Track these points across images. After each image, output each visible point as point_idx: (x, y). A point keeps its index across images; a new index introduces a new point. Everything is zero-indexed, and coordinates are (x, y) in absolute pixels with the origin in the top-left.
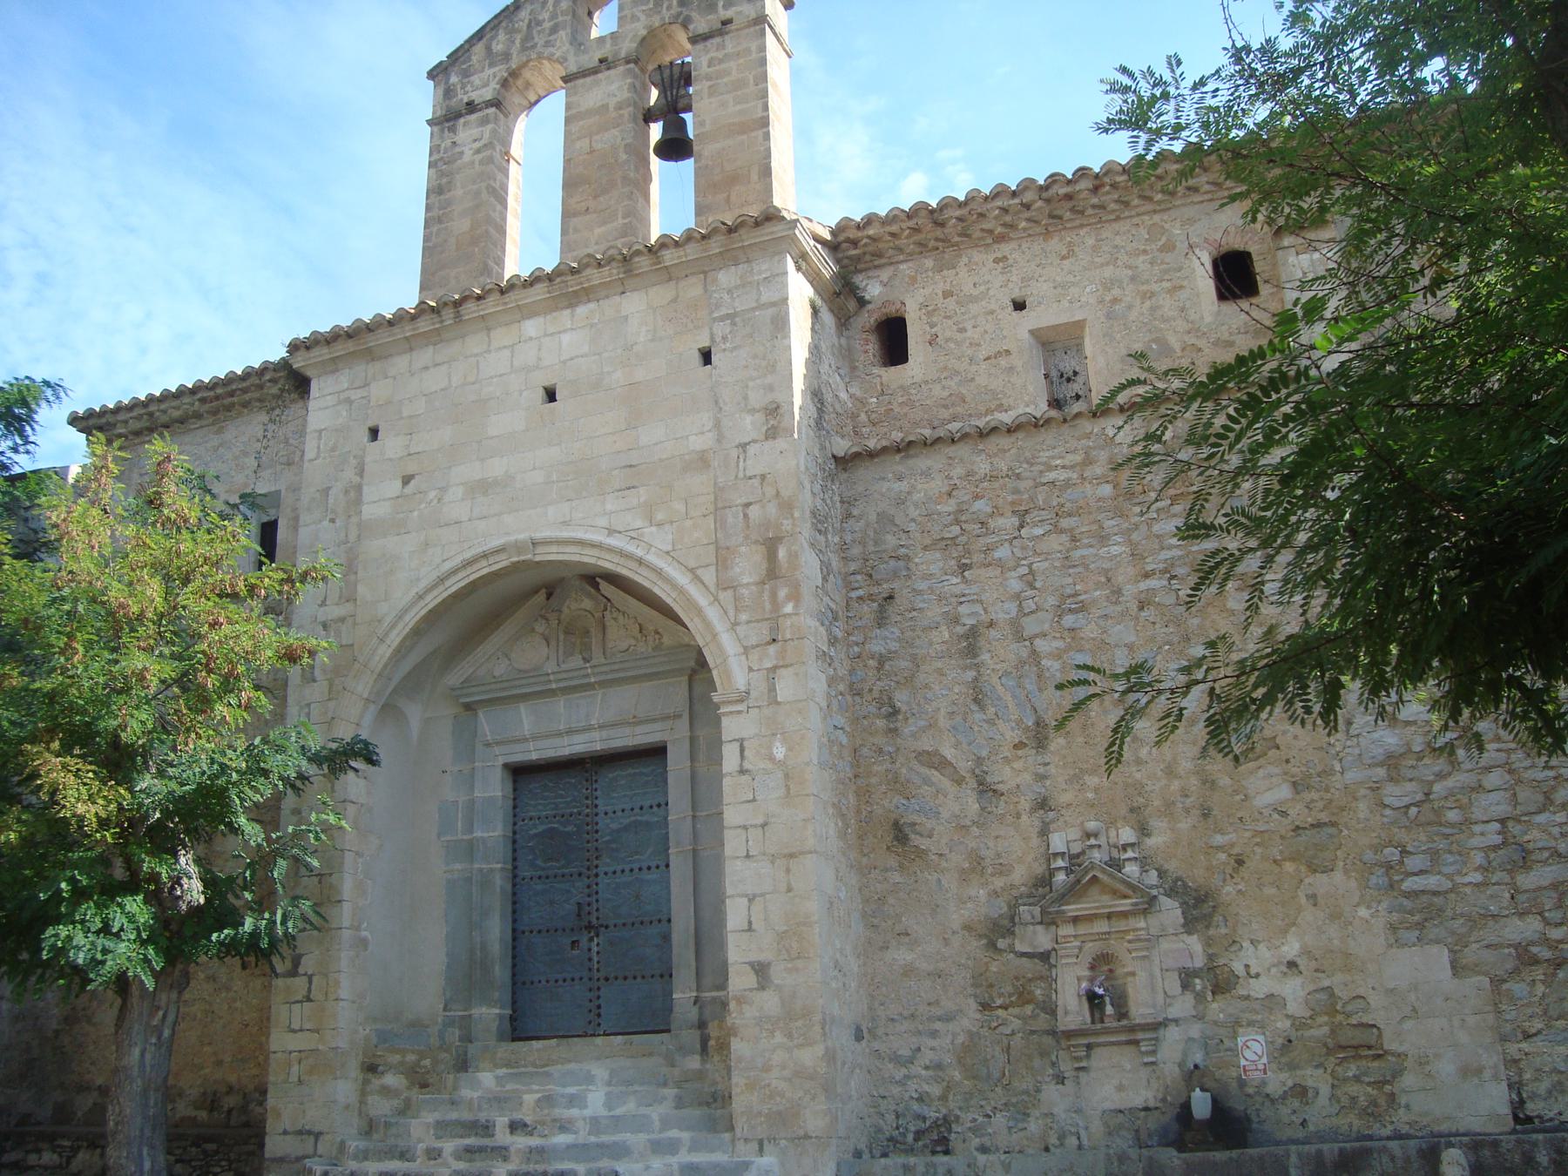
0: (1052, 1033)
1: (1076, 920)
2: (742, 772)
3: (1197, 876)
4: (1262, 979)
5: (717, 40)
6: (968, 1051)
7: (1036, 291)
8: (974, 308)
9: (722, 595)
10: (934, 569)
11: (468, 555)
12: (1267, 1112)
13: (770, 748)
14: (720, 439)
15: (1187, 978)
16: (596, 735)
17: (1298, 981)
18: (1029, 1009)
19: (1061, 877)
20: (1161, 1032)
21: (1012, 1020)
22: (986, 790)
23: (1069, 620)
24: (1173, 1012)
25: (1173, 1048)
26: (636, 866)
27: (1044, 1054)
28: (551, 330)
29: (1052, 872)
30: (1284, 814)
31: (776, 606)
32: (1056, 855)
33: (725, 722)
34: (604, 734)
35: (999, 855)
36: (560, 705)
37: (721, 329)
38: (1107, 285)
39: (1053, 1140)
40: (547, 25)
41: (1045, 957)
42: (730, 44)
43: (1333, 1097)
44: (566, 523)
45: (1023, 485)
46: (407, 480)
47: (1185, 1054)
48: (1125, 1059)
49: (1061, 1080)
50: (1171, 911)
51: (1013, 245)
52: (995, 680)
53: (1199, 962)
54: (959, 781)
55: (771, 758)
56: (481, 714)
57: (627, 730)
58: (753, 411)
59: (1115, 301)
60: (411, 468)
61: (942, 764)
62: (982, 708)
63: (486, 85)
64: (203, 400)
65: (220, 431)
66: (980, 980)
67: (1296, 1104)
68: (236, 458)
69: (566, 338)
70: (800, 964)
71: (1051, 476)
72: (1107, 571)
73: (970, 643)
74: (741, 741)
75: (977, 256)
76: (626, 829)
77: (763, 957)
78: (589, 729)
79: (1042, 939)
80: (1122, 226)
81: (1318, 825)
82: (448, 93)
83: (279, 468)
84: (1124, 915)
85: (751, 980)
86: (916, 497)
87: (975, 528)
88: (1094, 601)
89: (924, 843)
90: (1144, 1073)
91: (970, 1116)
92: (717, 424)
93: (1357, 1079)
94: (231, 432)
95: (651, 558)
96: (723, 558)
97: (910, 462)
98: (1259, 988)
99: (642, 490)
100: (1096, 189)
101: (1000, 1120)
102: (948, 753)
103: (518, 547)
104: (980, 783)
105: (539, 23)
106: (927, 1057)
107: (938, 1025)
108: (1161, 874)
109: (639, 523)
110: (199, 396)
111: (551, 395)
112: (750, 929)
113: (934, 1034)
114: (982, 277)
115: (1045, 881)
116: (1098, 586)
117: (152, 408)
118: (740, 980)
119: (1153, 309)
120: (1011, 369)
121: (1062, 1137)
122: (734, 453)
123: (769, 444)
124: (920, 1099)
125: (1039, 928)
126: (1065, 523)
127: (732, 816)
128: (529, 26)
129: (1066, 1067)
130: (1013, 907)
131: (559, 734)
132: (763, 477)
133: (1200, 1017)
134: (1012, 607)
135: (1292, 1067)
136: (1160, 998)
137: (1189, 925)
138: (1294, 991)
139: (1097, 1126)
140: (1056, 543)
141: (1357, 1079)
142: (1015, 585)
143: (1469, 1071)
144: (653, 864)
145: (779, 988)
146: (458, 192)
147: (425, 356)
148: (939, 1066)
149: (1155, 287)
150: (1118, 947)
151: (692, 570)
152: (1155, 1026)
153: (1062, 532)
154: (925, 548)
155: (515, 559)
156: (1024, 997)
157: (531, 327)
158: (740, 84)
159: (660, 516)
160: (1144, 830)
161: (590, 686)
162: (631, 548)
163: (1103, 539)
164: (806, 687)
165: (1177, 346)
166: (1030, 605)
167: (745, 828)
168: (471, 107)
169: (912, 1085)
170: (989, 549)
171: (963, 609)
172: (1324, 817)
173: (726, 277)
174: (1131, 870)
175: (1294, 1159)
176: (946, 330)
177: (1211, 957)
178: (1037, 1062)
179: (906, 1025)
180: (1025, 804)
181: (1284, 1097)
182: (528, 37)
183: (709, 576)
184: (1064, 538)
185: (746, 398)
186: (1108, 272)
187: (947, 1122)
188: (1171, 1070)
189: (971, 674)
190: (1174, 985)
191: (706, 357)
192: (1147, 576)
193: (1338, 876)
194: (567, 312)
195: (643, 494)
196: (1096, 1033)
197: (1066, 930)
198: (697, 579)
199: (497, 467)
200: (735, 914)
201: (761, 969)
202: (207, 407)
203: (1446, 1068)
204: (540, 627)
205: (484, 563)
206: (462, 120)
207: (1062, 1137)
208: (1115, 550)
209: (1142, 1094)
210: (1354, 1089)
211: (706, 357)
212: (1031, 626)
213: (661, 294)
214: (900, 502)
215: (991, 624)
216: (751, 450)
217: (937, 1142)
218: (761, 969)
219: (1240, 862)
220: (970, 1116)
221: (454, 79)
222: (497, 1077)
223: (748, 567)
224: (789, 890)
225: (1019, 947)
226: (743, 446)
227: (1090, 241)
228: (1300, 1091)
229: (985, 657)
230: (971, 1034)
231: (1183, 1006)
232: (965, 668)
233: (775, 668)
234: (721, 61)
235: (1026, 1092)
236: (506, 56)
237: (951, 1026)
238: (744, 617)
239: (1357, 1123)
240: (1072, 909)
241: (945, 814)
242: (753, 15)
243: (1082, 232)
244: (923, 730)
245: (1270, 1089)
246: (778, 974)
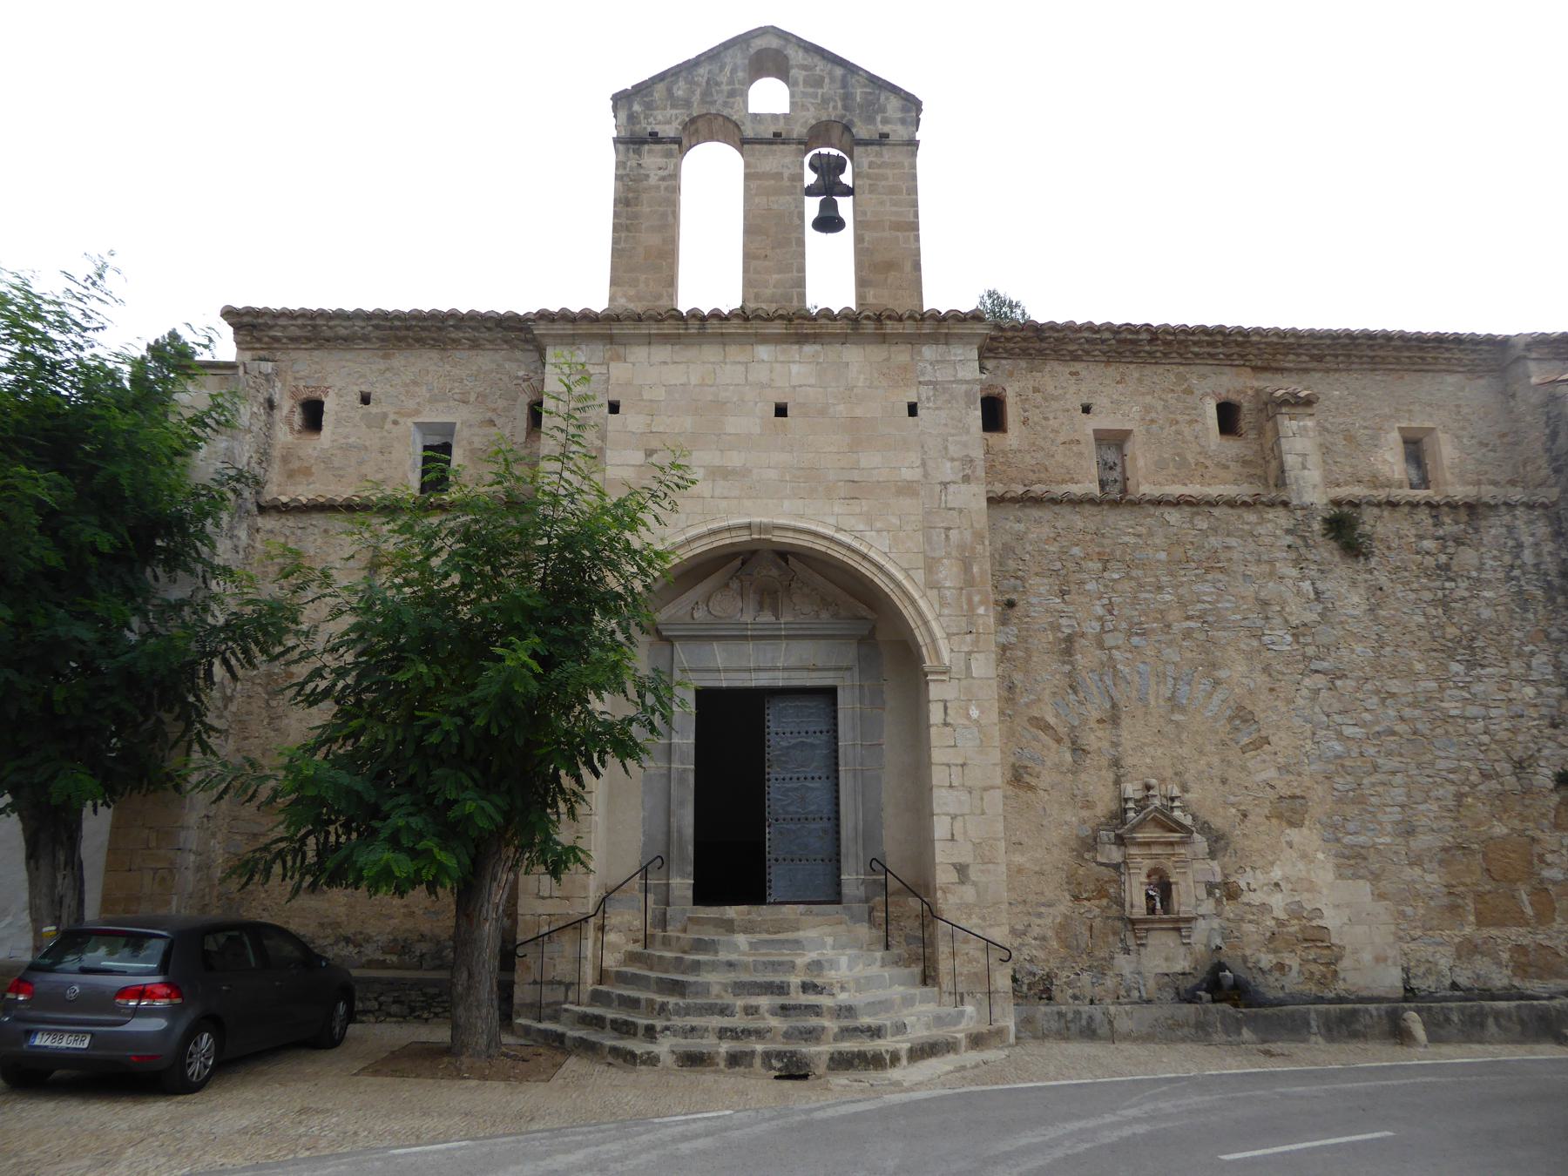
0: (1121, 919)
1: (1140, 844)
2: (946, 724)
3: (1217, 823)
4: (1259, 893)
5: (876, 148)
6: (1063, 928)
7: (1100, 402)
8: (1055, 405)
9: (929, 592)
10: (1043, 590)
11: (715, 526)
12: (1260, 979)
13: (967, 710)
14: (926, 475)
15: (1210, 888)
16: (780, 674)
17: (1279, 896)
18: (1104, 902)
19: (1131, 814)
20: (1193, 925)
21: (1093, 908)
22: (1078, 750)
23: (1135, 640)
24: (1202, 910)
25: (1203, 934)
26: (802, 776)
27: (1115, 933)
28: (781, 358)
29: (1125, 811)
30: (1273, 787)
31: (971, 607)
32: (1126, 800)
33: (932, 686)
34: (786, 674)
35: (1086, 795)
36: (750, 647)
37: (926, 391)
38: (1148, 409)
39: (1123, 993)
40: (725, 88)
41: (1116, 867)
42: (887, 154)
43: (1300, 972)
44: (801, 516)
45: (1106, 541)
46: (649, 453)
47: (1209, 940)
48: (1170, 940)
49: (1127, 951)
50: (1200, 843)
51: (1083, 365)
52: (1084, 674)
53: (1219, 879)
54: (1059, 741)
55: (968, 717)
56: (677, 645)
57: (805, 674)
58: (953, 460)
59: (1152, 421)
60: (655, 444)
61: (1047, 728)
62: (1076, 692)
63: (669, 122)
64: (376, 327)
65: (386, 357)
66: (1071, 879)
67: (1277, 974)
68: (407, 385)
69: (795, 368)
70: (991, 866)
71: (1126, 539)
72: (1161, 612)
73: (1067, 646)
74: (945, 702)
76: (794, 747)
77: (962, 860)
78: (775, 669)
79: (1115, 855)
80: (1160, 369)
81: (1294, 797)
82: (632, 118)
83: (452, 403)
84: (1172, 844)
85: (953, 877)
86: (1031, 536)
87: (1071, 566)
88: (1153, 630)
89: (1033, 782)
90: (1182, 950)
91: (1065, 974)
92: (924, 464)
93: (1315, 961)
94: (398, 360)
95: (872, 554)
96: (931, 565)
97: (1028, 511)
98: (1256, 898)
99: (864, 502)
100: (1150, 341)
101: (1086, 977)
102: (1052, 720)
103: (762, 528)
104: (1073, 743)
105: (717, 84)
106: (1036, 931)
107: (1042, 909)
108: (1195, 818)
109: (861, 527)
110: (374, 322)
111: (781, 411)
112: (952, 839)
113: (1040, 915)
115: (1120, 816)
116: (1156, 620)
117: (320, 322)
118: (944, 876)
119: (1178, 433)
120: (1080, 454)
121: (1128, 991)
122: (938, 488)
123: (964, 487)
124: (1031, 961)
125: (1114, 847)
126: (1134, 573)
127: (937, 755)
128: (708, 82)
129: (1131, 942)
130: (1096, 831)
131: (749, 670)
132: (961, 511)
133: (1218, 915)
134: (1097, 625)
135: (1275, 951)
136: (1193, 900)
137: (1212, 855)
138: (1278, 902)
139: (1151, 983)
140: (1127, 586)
141: (1315, 961)
142: (1100, 611)
143: (1380, 959)
144: (816, 776)
145: (975, 884)
146: (646, 209)
147: (662, 353)
148: (1044, 938)
149: (1179, 417)
150: (1168, 864)
151: (906, 570)
152: (1188, 920)
153: (1132, 578)
154: (1036, 574)
155: (756, 536)
156: (1101, 893)
157: (764, 352)
158: (893, 190)
159: (879, 525)
160: (1185, 789)
161: (778, 637)
162: (856, 544)
163: (1160, 589)
164: (984, 666)
165: (1192, 461)
166: (1109, 626)
167: (948, 765)
168: (655, 138)
169: (1025, 951)
170: (1083, 583)
171: (1064, 622)
172: (1298, 792)
173: (929, 352)
174: (1177, 814)
175: (1313, 1015)
176: (1035, 416)
177: (1226, 876)
178: (1111, 939)
179: (1020, 908)
180: (1104, 762)
181: (1270, 971)
183: (919, 576)
184: (1133, 584)
185: (946, 448)
186: (1148, 399)
187: (1049, 977)
188: (1199, 948)
189: (1068, 668)
190: (1203, 894)
191: (913, 410)
192: (1189, 618)
193: (1305, 831)
194: (796, 347)
195: (865, 505)
196: (1153, 921)
197: (1133, 851)
198: (909, 576)
199: (735, 459)
200: (941, 828)
201: (961, 869)
202: (378, 333)
203: (1367, 957)
204: (735, 585)
205: (727, 535)
206: (646, 147)
207: (1128, 991)
208: (1168, 597)
209: (1182, 965)
210: (1313, 967)
211: (913, 410)
212: (1109, 640)
213: (877, 353)
214: (1020, 538)
215: (1083, 635)
216: (951, 488)
217: (1042, 992)
218: (961, 869)
219: (1245, 816)
220: (1065, 974)
221: (636, 108)
222: (751, 944)
223: (949, 574)
224: (983, 813)
225: (1099, 859)
226: (945, 485)
227: (1136, 375)
228: (1281, 967)
229: (1079, 657)
230: (1066, 916)
231: (1208, 906)
232: (1064, 663)
233: (969, 653)
234: (880, 167)
235: (1104, 959)
236: (687, 104)
237: (1051, 910)
238: (946, 611)
239: (1314, 989)
240: (1139, 836)
241: (1049, 763)
242: (906, 138)
243: (1132, 367)
244: (1033, 702)
245: (1262, 965)
246: (973, 874)
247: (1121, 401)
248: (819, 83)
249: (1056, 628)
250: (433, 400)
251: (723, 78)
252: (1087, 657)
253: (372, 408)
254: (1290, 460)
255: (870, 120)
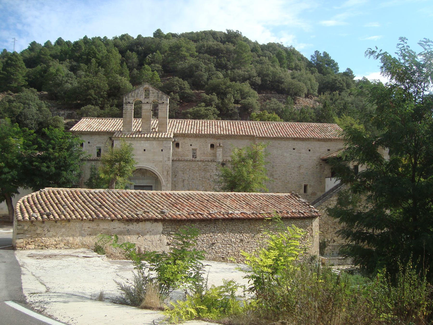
7: (193, 144)
37: (164, 148)
73: (183, 181)
75: (187, 138)
94: (93, 137)
96: (163, 172)
111: (145, 150)
114: (188, 141)
157: (143, 142)
158: (164, 112)
173: (164, 142)
182: (137, 95)
183: (161, 173)
191: (162, 150)
211: (162, 150)
214: (178, 166)
223: (165, 173)
236: (134, 97)
247: (197, 144)
248: (154, 93)
249: (182, 178)
250: (98, 143)
251: (139, 92)
252: (186, 182)
253: (90, 144)
254: (218, 155)
255: (161, 100)
